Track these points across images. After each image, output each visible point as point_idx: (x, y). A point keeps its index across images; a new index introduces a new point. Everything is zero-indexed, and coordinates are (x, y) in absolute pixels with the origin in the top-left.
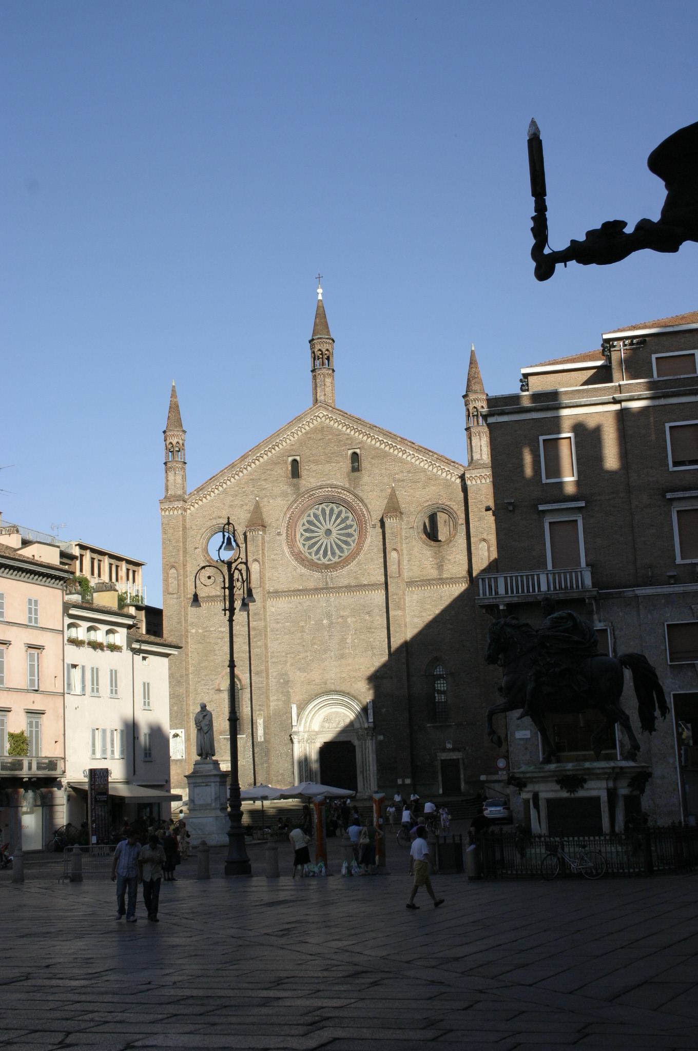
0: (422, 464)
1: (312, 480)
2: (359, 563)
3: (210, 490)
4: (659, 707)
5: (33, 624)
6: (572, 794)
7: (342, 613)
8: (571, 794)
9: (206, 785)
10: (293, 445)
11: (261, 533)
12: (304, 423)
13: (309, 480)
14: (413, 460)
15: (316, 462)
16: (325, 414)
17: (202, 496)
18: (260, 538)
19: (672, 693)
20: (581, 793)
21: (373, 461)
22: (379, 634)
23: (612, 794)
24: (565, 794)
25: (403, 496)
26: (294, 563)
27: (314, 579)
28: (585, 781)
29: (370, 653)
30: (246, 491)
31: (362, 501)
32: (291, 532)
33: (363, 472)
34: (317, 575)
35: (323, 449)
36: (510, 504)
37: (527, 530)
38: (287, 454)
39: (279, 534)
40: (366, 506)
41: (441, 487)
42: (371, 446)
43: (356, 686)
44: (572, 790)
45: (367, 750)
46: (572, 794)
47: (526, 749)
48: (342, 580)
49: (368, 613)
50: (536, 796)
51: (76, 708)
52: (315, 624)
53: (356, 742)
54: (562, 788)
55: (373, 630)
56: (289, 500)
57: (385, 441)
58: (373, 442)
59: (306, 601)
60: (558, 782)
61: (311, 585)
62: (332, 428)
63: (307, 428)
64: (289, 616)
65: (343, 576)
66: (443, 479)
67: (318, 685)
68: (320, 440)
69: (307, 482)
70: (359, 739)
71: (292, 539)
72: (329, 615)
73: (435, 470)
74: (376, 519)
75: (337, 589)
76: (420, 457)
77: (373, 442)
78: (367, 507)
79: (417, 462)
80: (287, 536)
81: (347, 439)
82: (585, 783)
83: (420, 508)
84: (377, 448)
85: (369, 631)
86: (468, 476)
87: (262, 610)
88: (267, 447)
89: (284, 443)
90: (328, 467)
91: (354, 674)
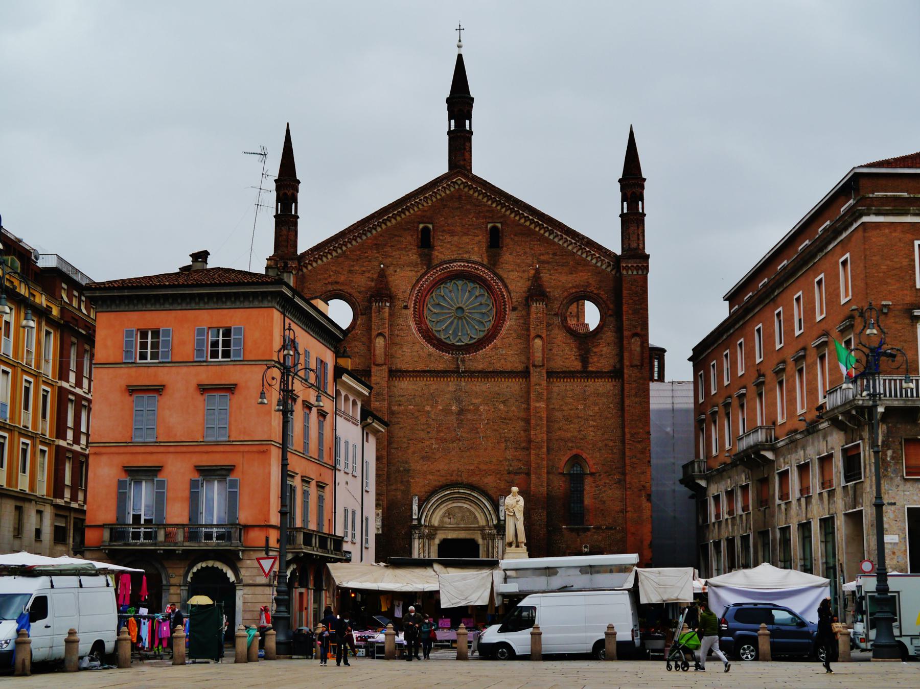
0: (570, 248)
1: (446, 252)
2: (495, 347)
3: (326, 251)
7: (474, 401)
10: (425, 211)
11: (388, 305)
12: (440, 188)
13: (441, 253)
14: (561, 243)
15: (452, 233)
16: (464, 181)
17: (317, 256)
18: (387, 310)
19: (906, 507)
21: (516, 239)
22: (515, 426)
25: (546, 277)
26: (422, 341)
27: (444, 360)
29: (503, 445)
30: (368, 256)
31: (501, 279)
32: (420, 307)
33: (505, 249)
34: (447, 356)
35: (460, 219)
36: (885, 306)
37: (900, 334)
38: (418, 220)
39: (406, 307)
40: (506, 286)
41: (589, 274)
42: (514, 221)
43: (486, 480)
45: (495, 550)
47: (894, 553)
48: (476, 364)
49: (503, 402)
52: (442, 410)
53: (480, 541)
55: (508, 421)
56: (419, 271)
57: (531, 217)
58: (517, 218)
59: (434, 385)
61: (440, 366)
62: (471, 196)
63: (443, 195)
64: (414, 399)
65: (479, 360)
66: (592, 266)
67: (442, 476)
68: (457, 208)
69: (441, 253)
70: (483, 538)
71: (419, 313)
72: (458, 399)
73: (584, 256)
74: (517, 301)
75: (472, 374)
76: (569, 239)
77: (517, 218)
78: (508, 289)
79: (565, 245)
80: (414, 311)
81: (488, 211)
83: (565, 294)
84: (521, 225)
85: (503, 422)
86: (624, 265)
87: (387, 389)
88: (394, 211)
89: (416, 209)
90: (466, 239)
91: (482, 467)
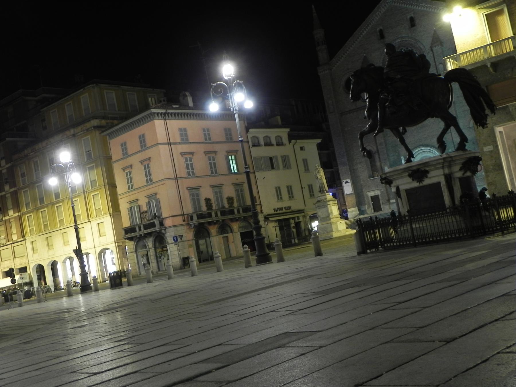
4: (487, 107)
5: (208, 141)
6: (421, 183)
8: (420, 184)
9: (325, 207)
20: (427, 182)
23: (449, 178)
24: (416, 184)
28: (427, 172)
44: (420, 180)
46: (421, 183)
47: (492, 157)
50: (398, 188)
51: (263, 179)
54: (413, 180)
60: (410, 176)
82: (428, 174)
